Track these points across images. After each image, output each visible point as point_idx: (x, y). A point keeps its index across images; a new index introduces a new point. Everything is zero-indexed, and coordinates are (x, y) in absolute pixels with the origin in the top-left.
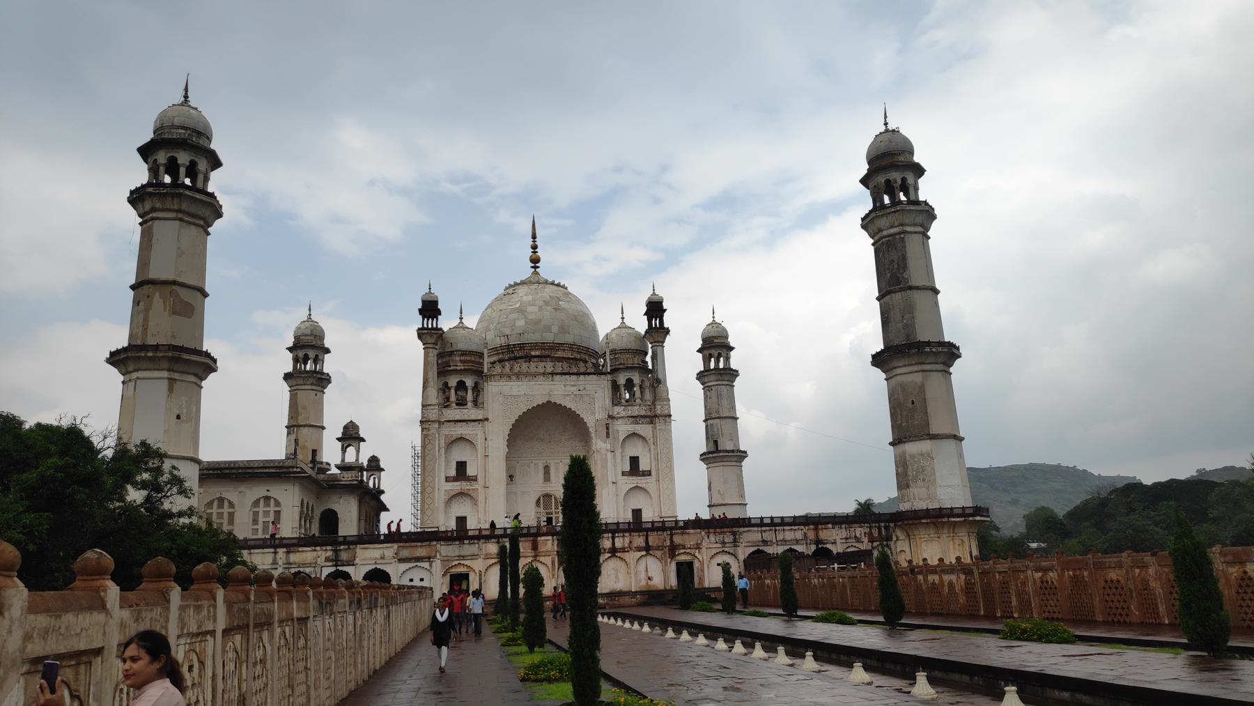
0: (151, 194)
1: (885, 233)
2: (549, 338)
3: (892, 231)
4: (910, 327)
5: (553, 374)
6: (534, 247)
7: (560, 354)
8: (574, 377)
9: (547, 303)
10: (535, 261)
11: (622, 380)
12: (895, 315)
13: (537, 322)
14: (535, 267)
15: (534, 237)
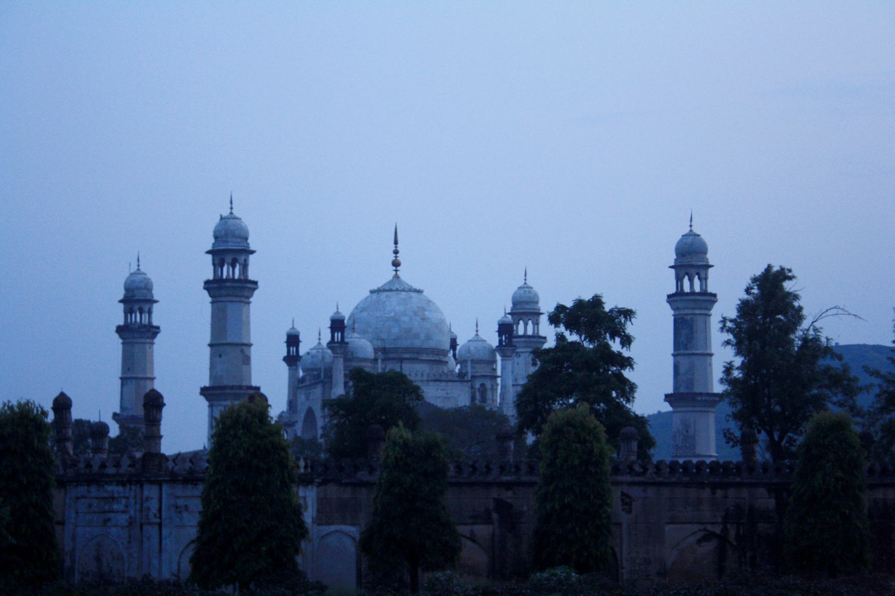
0: (228, 287)
1: (682, 312)
2: (417, 343)
3: (686, 311)
4: (690, 383)
5: (428, 381)
6: (396, 252)
7: (424, 357)
8: (443, 384)
9: (415, 313)
10: (396, 264)
11: (477, 386)
12: (682, 370)
13: (409, 330)
14: (396, 271)
15: (396, 243)
